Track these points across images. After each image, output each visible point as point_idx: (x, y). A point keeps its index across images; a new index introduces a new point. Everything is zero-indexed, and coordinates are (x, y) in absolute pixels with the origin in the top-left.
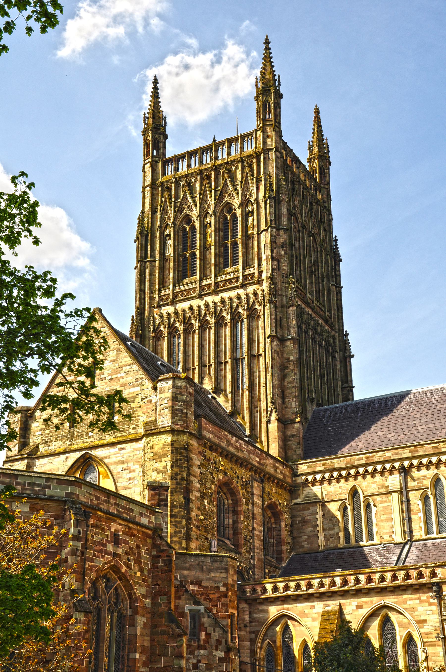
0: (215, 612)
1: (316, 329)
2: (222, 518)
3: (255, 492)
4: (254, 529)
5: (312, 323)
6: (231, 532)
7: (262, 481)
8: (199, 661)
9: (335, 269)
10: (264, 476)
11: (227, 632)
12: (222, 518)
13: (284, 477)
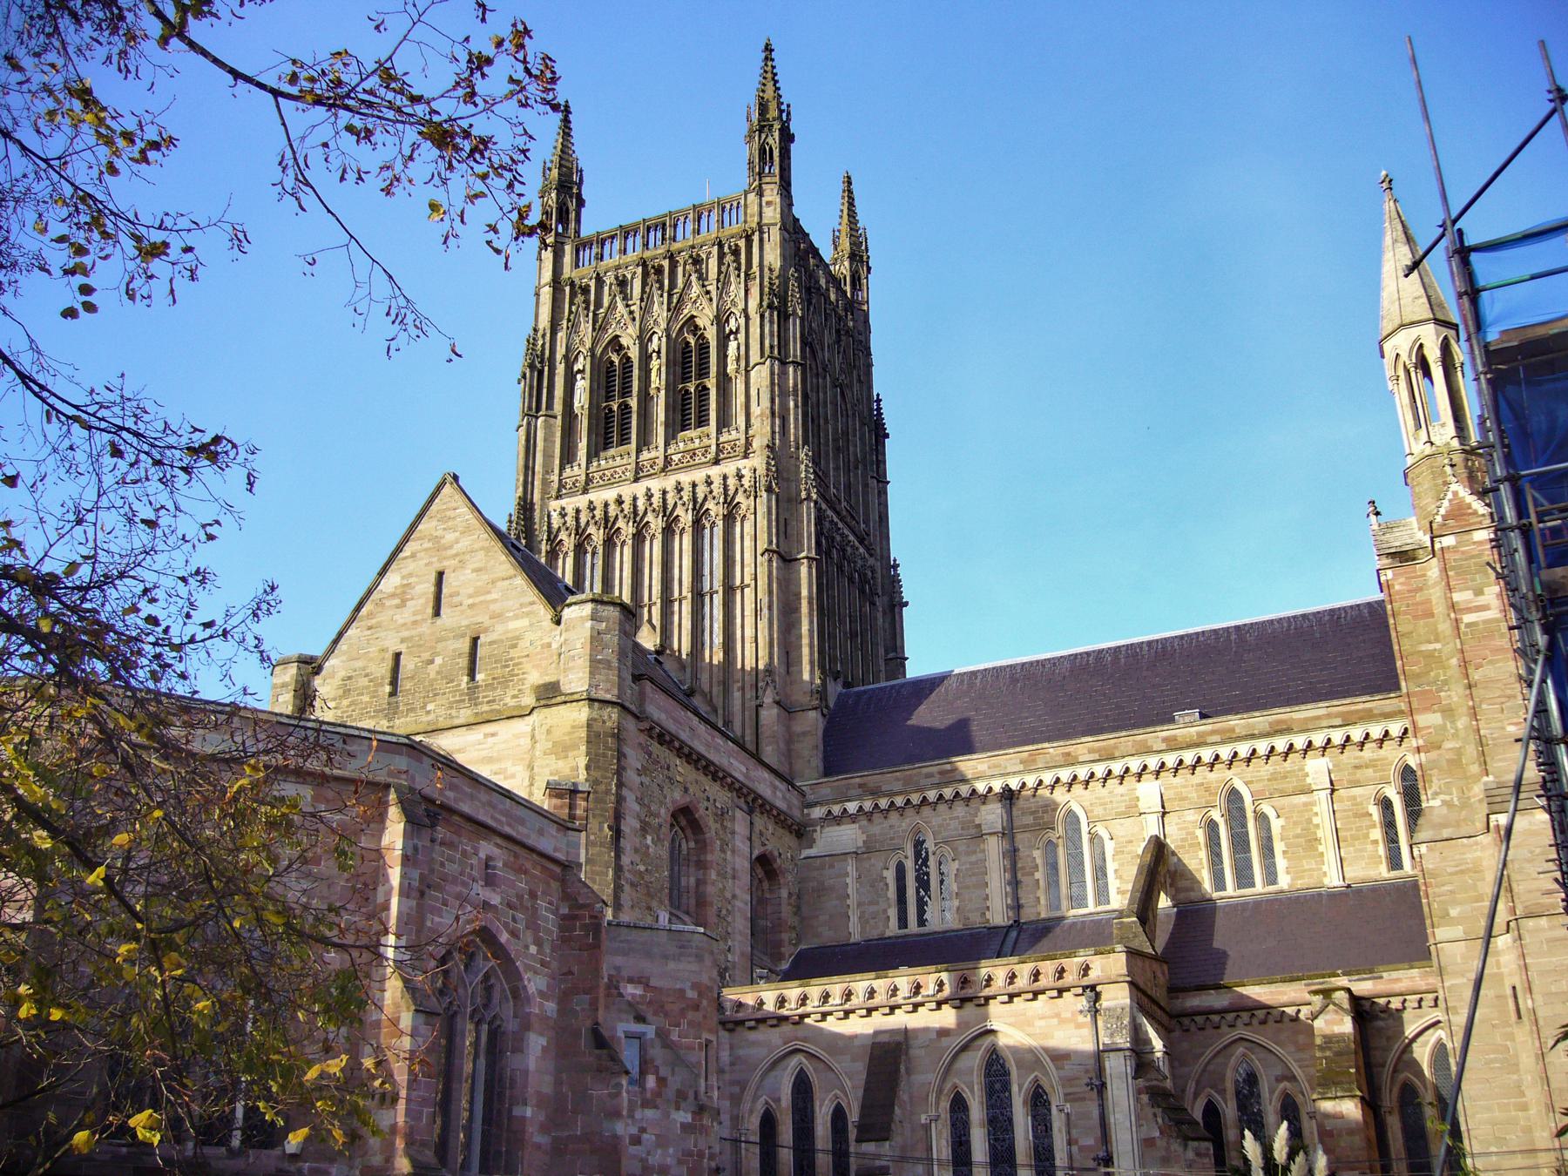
0: (674, 1037)
1: (844, 550)
2: (676, 875)
3: (738, 828)
4: (734, 896)
5: (838, 538)
6: (693, 901)
7: (750, 812)
8: (643, 1130)
9: (877, 450)
10: (754, 800)
11: (698, 1076)
12: (676, 875)
13: (790, 807)
